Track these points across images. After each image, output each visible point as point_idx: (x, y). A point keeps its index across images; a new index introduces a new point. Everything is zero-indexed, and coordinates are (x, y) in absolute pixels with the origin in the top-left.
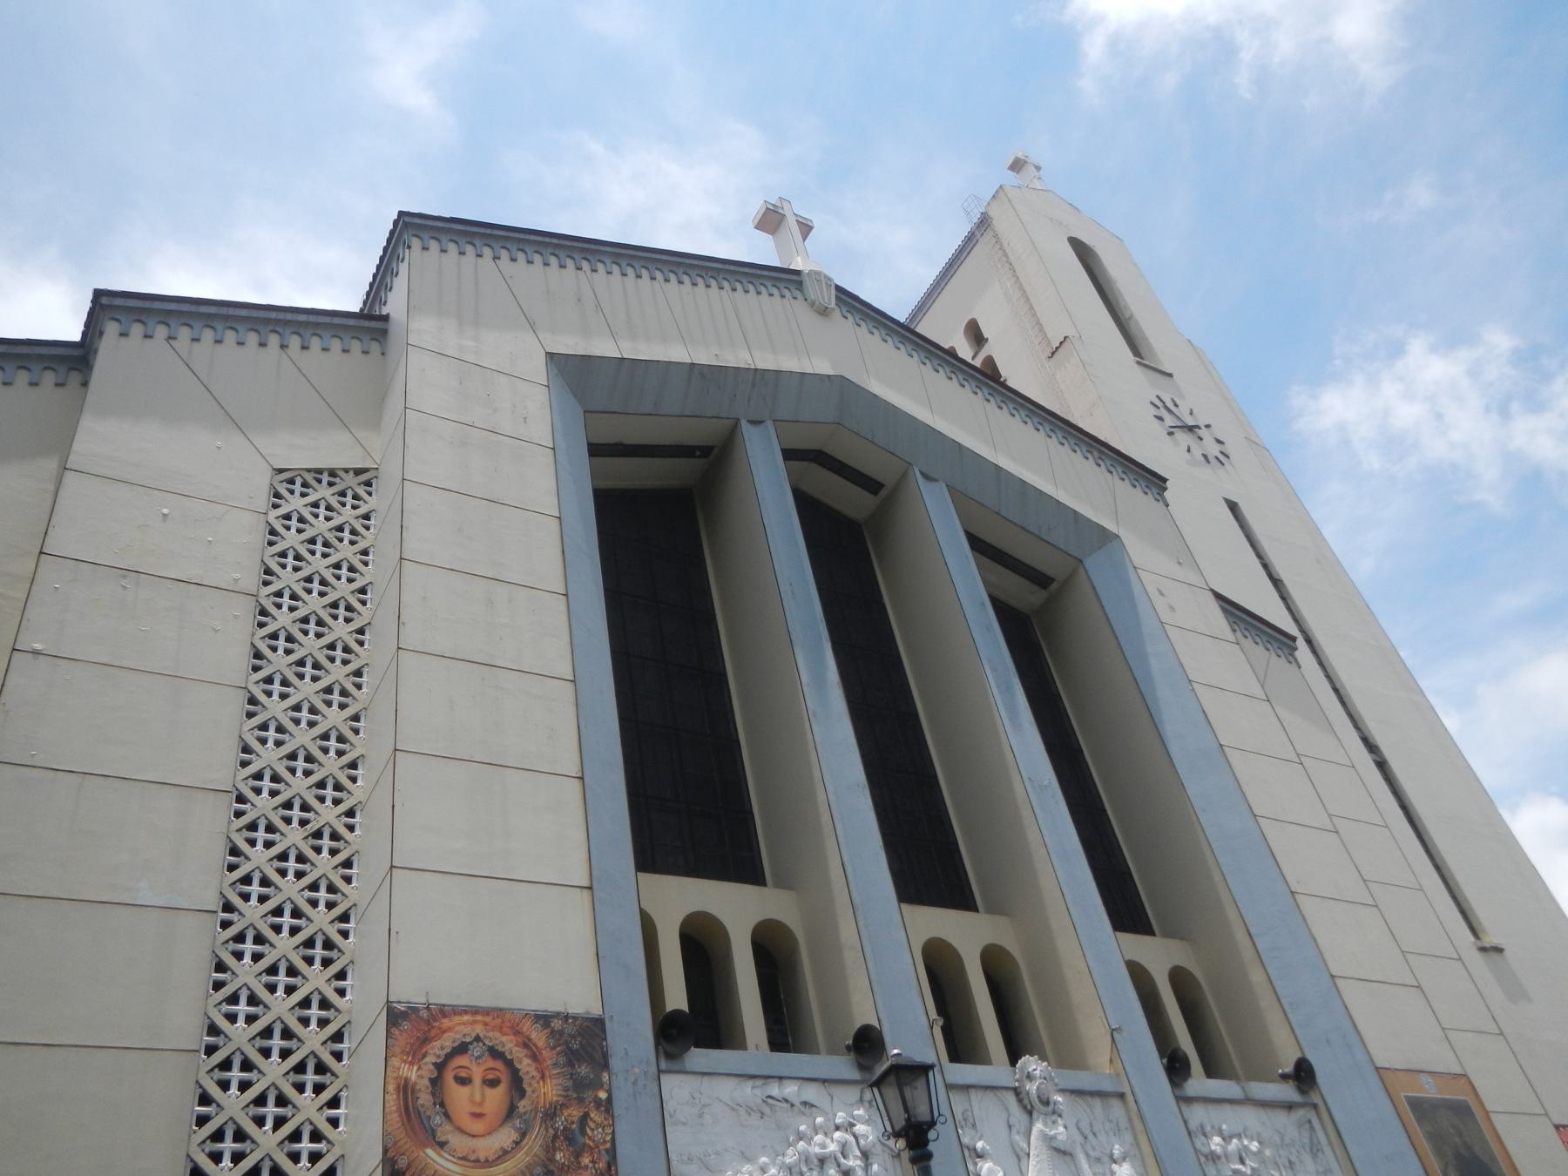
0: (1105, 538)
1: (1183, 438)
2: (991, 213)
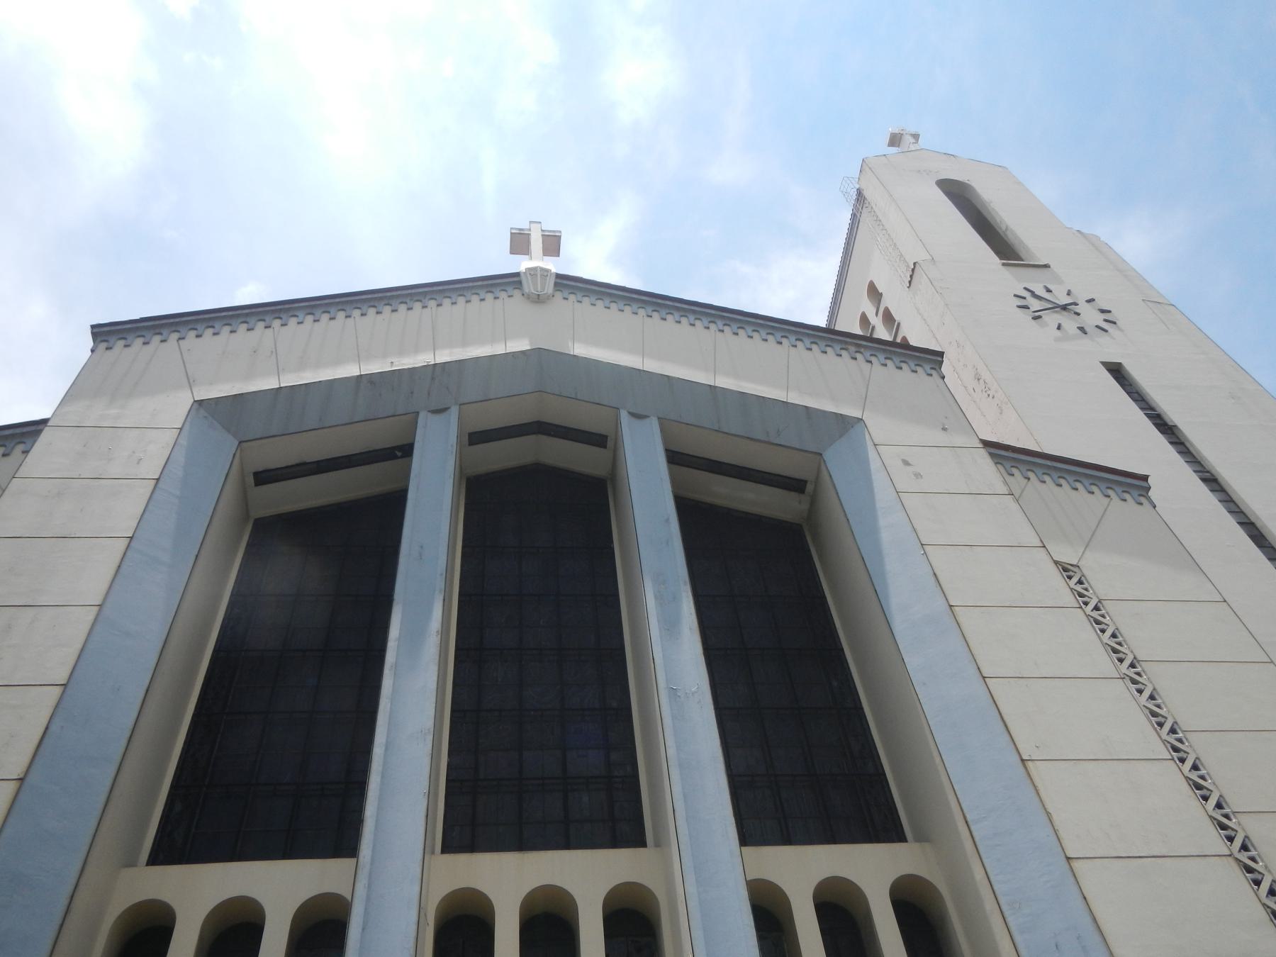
0: (844, 425)
1: (1052, 319)
2: (863, 187)
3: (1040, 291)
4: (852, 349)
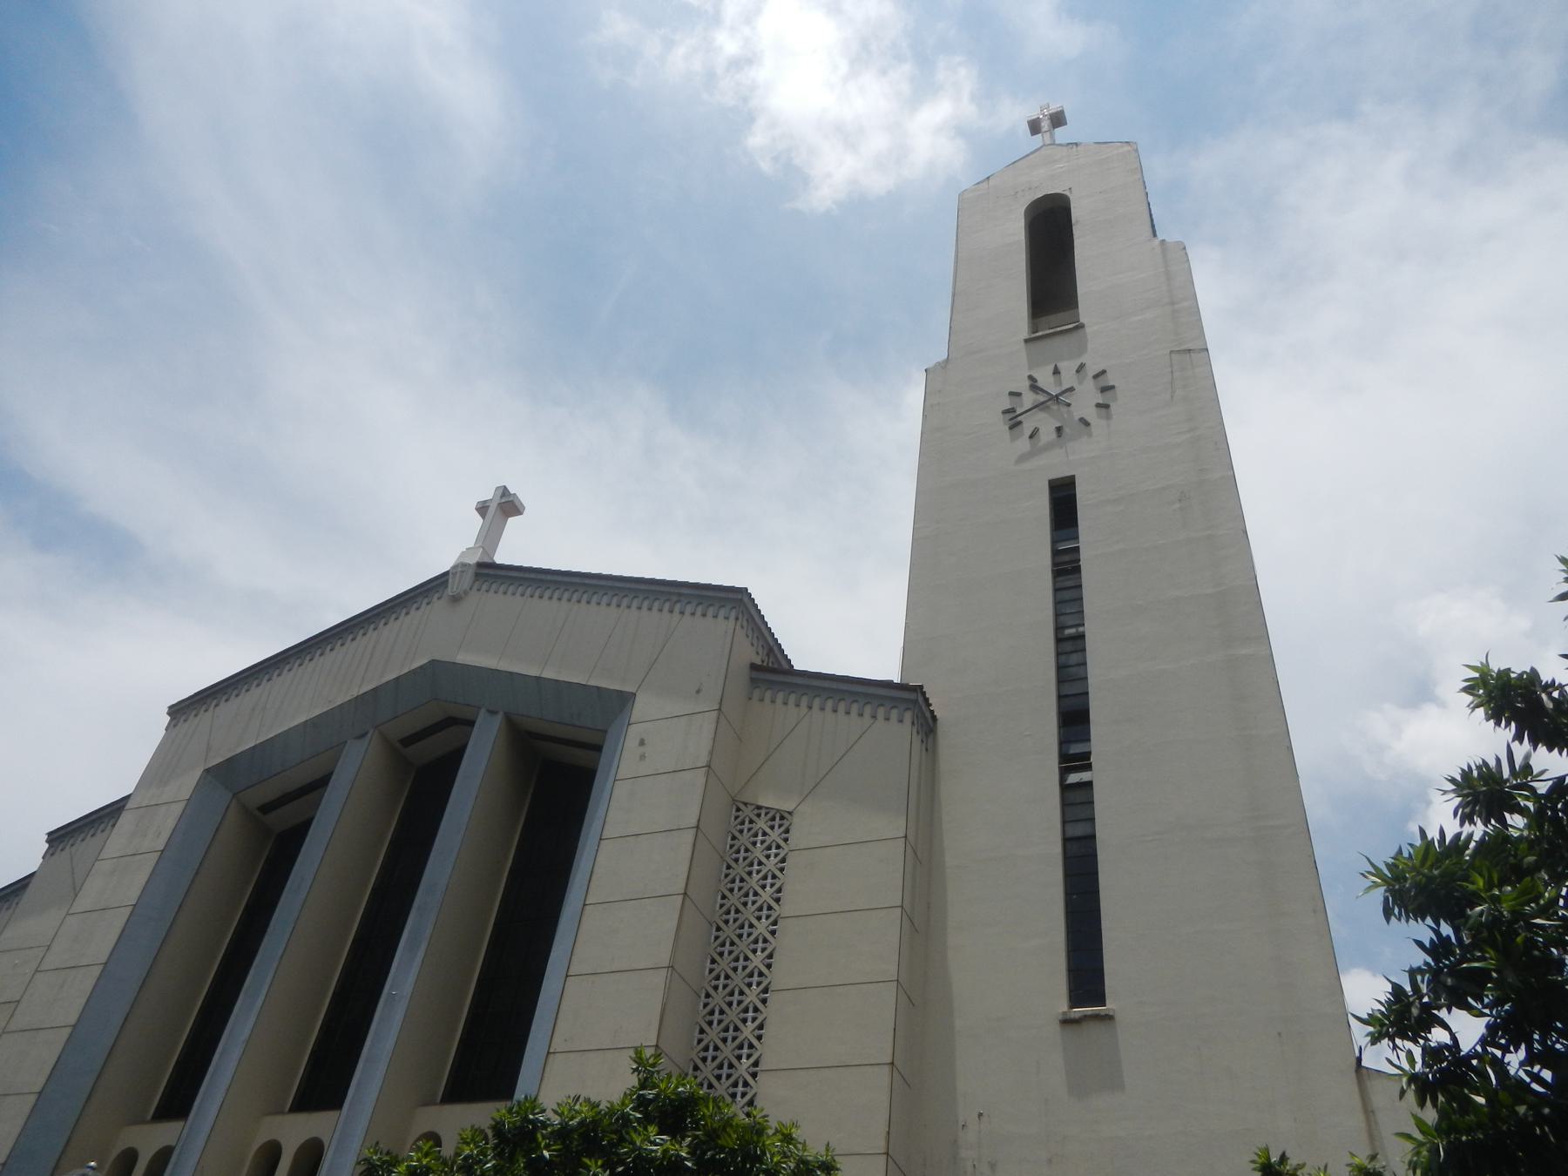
4: (675, 598)
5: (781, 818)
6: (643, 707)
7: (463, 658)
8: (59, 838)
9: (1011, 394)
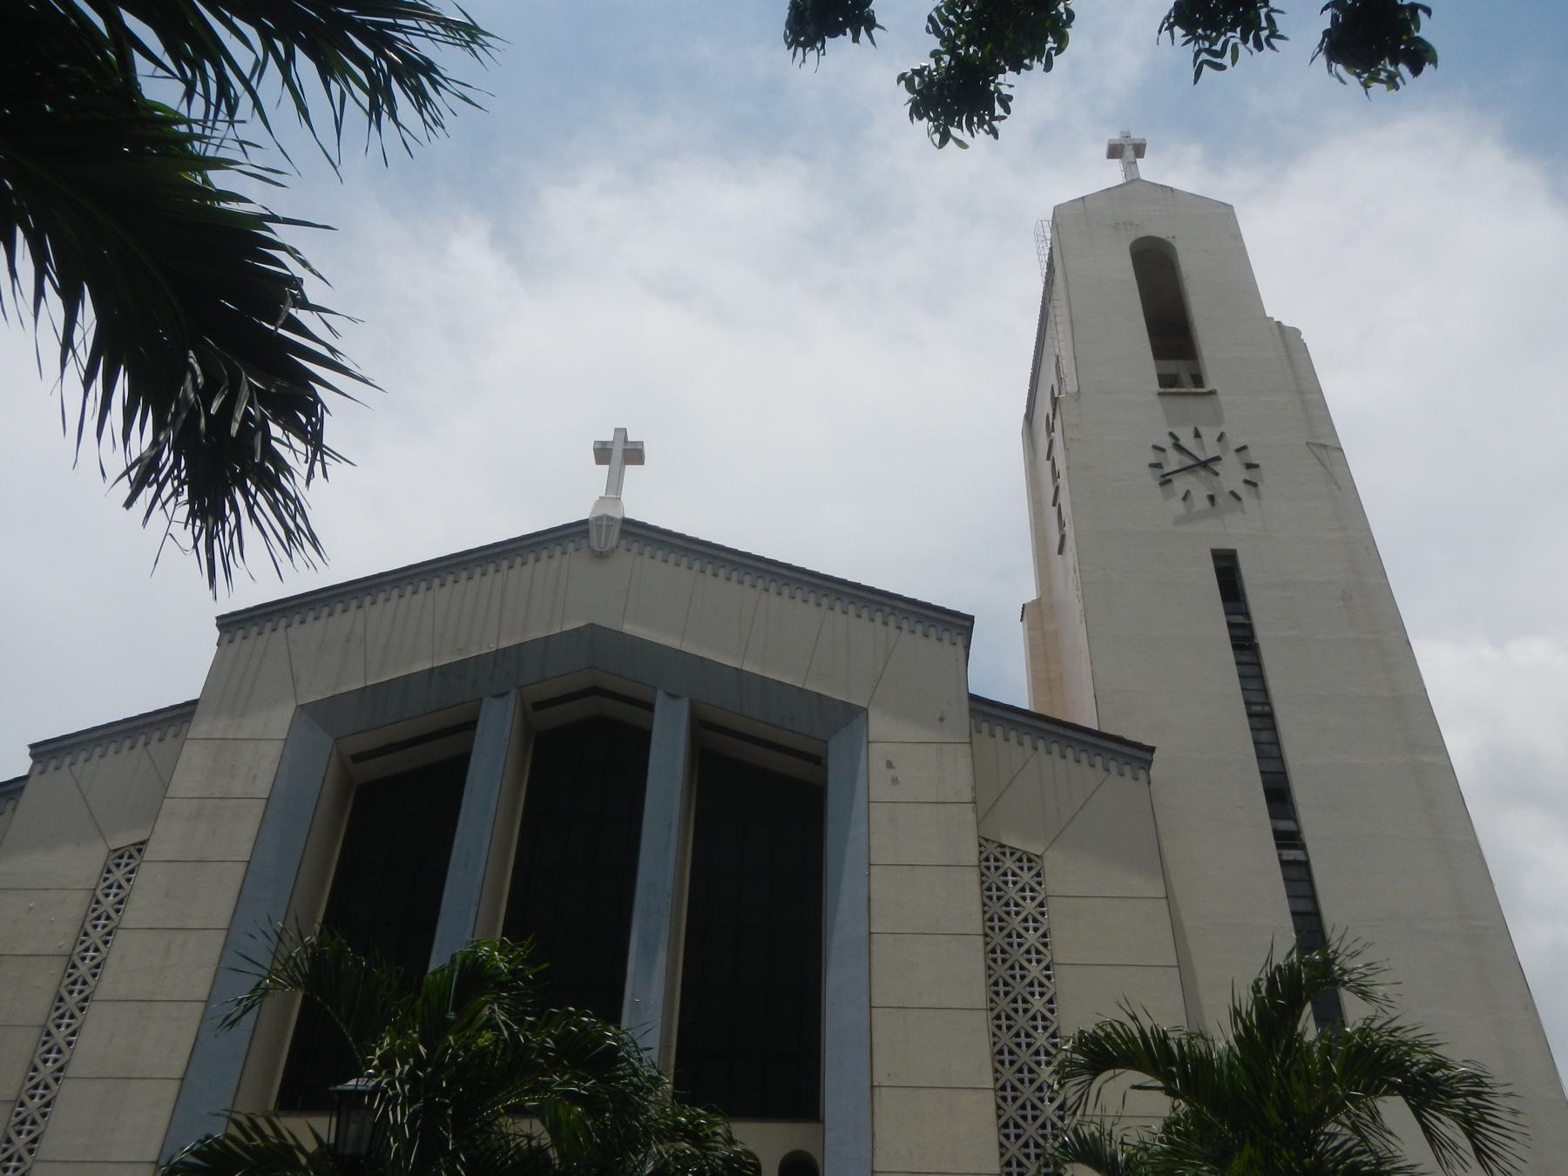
0: (852, 715)
3: (1187, 440)
4: (887, 610)
5: (1029, 860)
6: (879, 725)
7: (629, 628)
8: (41, 751)
9: (1155, 447)
